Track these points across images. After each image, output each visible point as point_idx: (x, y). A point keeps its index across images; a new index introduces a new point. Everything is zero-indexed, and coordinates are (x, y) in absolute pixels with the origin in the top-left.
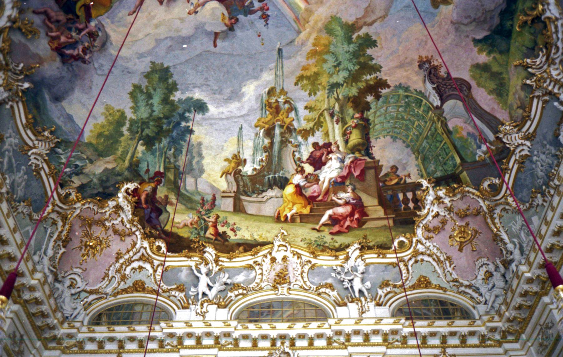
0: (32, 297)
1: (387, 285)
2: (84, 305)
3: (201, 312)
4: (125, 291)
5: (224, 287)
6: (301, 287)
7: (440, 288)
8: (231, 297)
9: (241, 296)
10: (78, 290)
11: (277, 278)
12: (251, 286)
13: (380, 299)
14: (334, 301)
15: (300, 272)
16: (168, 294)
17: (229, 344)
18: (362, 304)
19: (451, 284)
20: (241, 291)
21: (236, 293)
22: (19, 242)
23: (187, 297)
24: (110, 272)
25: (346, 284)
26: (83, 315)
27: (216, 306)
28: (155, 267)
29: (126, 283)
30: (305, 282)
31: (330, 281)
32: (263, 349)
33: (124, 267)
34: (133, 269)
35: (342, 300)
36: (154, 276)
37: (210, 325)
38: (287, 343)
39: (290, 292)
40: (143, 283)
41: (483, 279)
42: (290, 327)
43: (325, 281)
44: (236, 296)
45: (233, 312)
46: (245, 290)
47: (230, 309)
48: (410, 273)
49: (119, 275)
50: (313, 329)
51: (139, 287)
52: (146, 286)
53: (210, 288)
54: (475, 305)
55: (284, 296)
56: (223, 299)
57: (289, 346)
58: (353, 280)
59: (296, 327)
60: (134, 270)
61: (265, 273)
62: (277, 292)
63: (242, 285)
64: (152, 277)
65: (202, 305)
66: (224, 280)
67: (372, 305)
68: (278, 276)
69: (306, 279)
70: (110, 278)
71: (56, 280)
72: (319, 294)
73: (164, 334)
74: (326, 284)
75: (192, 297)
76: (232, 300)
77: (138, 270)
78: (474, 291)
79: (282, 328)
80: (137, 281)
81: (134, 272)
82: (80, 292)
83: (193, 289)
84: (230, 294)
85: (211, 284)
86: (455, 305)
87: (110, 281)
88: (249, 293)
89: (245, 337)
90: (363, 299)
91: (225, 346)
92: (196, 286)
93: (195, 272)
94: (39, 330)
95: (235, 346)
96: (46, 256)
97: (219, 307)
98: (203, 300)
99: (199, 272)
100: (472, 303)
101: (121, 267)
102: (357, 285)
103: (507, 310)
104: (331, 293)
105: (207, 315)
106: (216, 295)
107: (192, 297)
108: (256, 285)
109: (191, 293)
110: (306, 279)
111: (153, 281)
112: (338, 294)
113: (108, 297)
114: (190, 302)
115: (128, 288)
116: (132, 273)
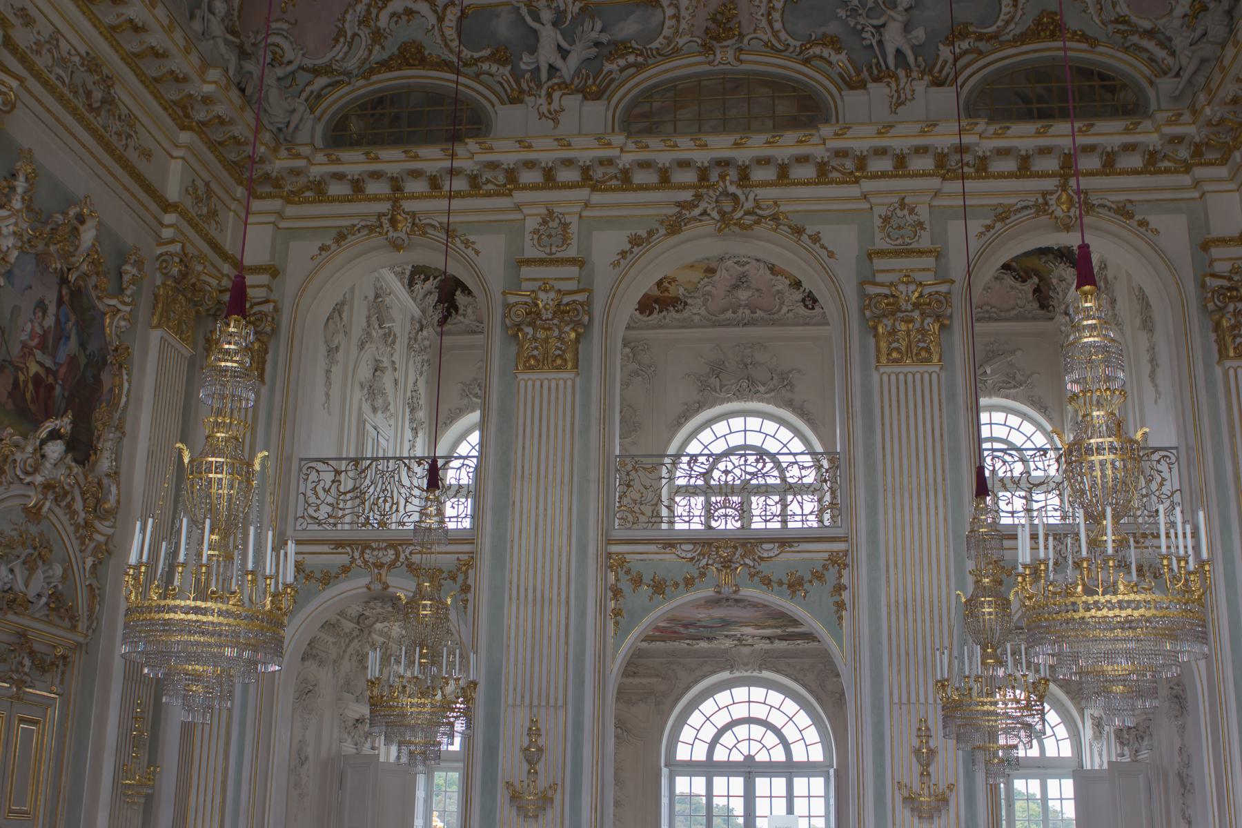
0: (211, 116)
1: (964, 35)
2: (306, 100)
3: (550, 112)
4: (385, 65)
5: (594, 51)
6: (766, 44)
7: (1084, 38)
8: (611, 72)
9: (632, 70)
10: (290, 68)
11: (712, 26)
12: (655, 45)
13: (942, 68)
14: (840, 75)
15: (763, 10)
16: (474, 69)
17: (611, 179)
18: (898, 85)
19: (1111, 28)
20: (631, 59)
21: (622, 62)
22: (166, 22)
23: (517, 75)
24: (347, 25)
25: (869, 37)
26: (310, 123)
27: (580, 96)
28: (439, 10)
29: (383, 48)
30: (775, 34)
31: (832, 28)
32: (683, 187)
33: (374, 11)
34: (394, 14)
35: (859, 72)
36: (441, 30)
37: (569, 145)
38: (733, 174)
39: (743, 57)
40: (420, 48)
41: (1185, 16)
42: (737, 145)
43: (824, 29)
44: (622, 70)
45: (617, 106)
46: (641, 54)
47: (609, 101)
48: (1020, 6)
49: (367, 31)
50: (788, 145)
51: (411, 55)
52: (426, 53)
53: (564, 54)
54: (1153, 78)
55: (729, 67)
56: (595, 78)
57: (736, 179)
58: (884, 25)
59: (750, 143)
60: (395, 19)
61: (683, 13)
62: (711, 57)
63: (635, 45)
64: (436, 32)
65: (549, 96)
66: (594, 35)
67: (920, 86)
68: (714, 20)
69: (778, 26)
70: (349, 39)
71: (243, 54)
72: (806, 62)
73: (476, 163)
74: (825, 35)
75: (528, 75)
76: (613, 80)
77: (404, 18)
78: (1160, 44)
79: (720, 146)
80: (405, 44)
81: (396, 23)
82: (293, 73)
83: (526, 58)
84: (608, 67)
85: (565, 45)
86: (1114, 79)
87: (351, 44)
88: (650, 61)
89: (644, 165)
90: (901, 73)
91: (604, 182)
92: (533, 50)
93: (528, 19)
94: (234, 168)
95: (623, 183)
96: (214, 14)
97: (585, 98)
98: (550, 83)
99: (537, 19)
100: (1147, 72)
101: (368, 11)
102: (893, 38)
103: (1209, 104)
104: (834, 58)
105: (562, 117)
106: (579, 70)
107: (528, 75)
108: (664, 41)
109: (523, 66)
110: (778, 26)
111: (439, 40)
112: (850, 60)
113: (353, 80)
114: (524, 86)
115: (391, 58)
116: (393, 26)
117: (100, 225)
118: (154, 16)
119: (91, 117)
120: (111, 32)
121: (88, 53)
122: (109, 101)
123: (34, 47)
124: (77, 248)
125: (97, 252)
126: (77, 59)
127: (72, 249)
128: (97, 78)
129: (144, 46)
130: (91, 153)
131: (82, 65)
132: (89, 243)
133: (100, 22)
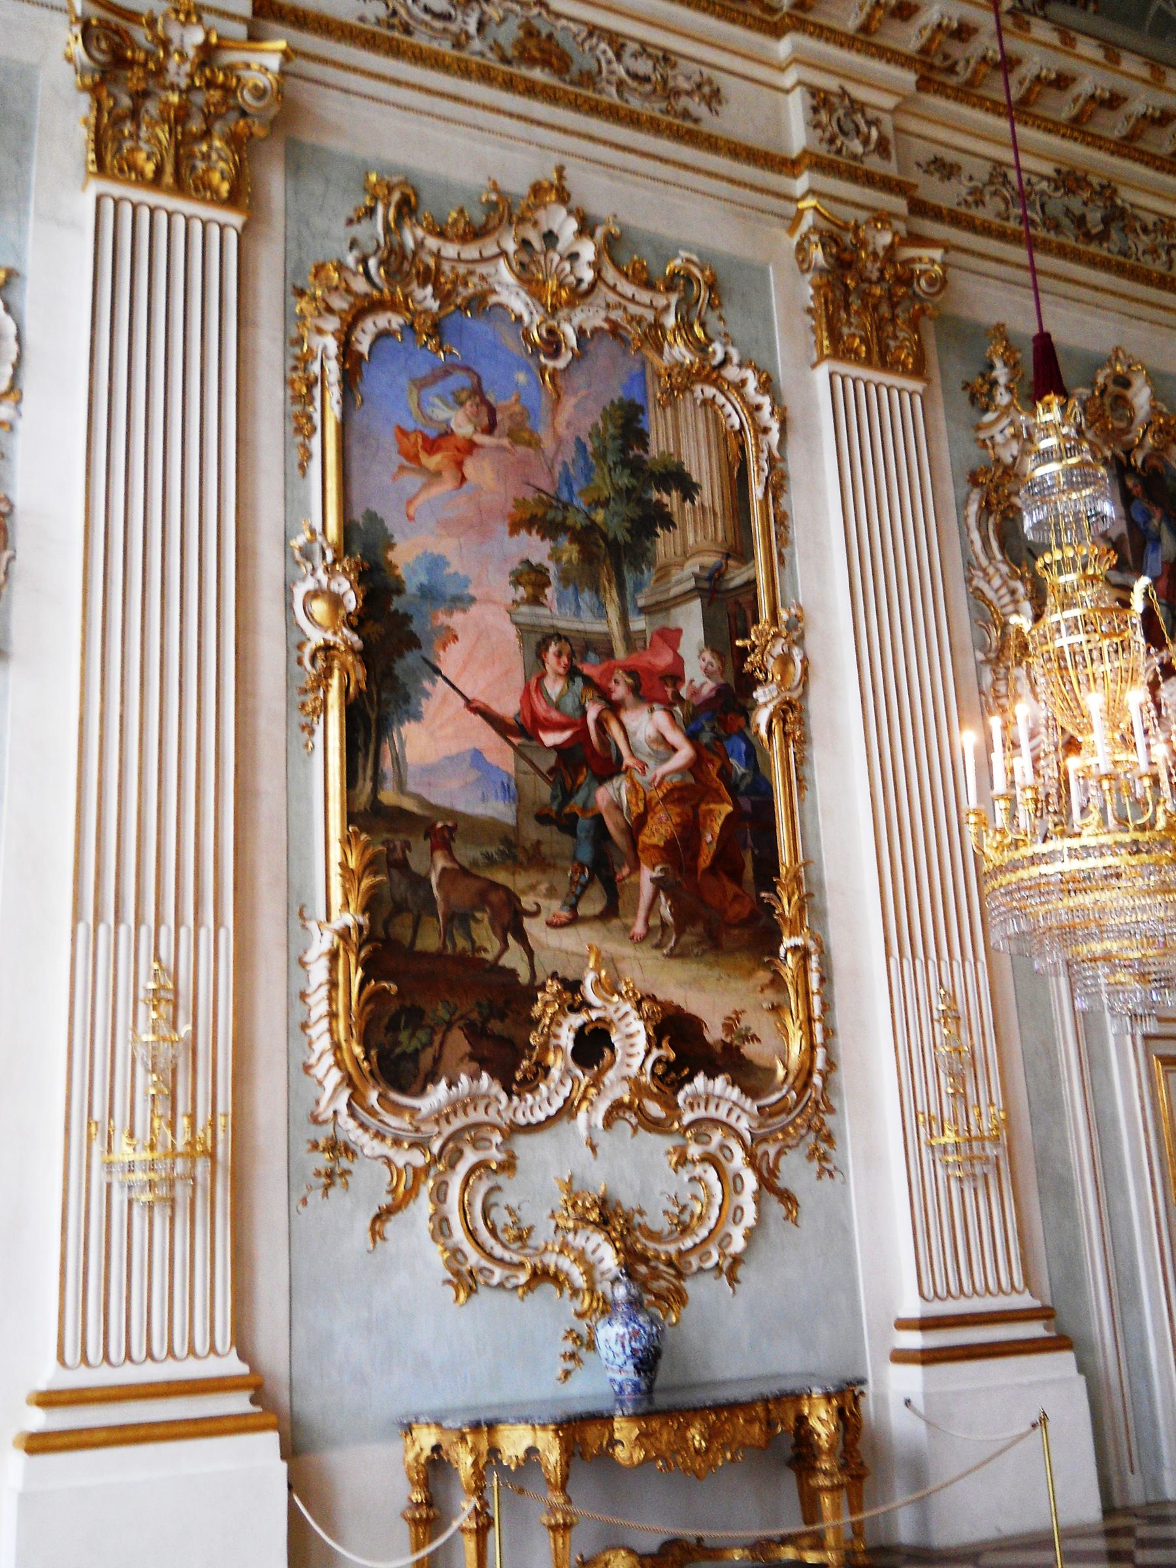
117: (1154, 378)
118: (1125, 74)
119: (1093, 248)
120: (1076, 128)
121: (1058, 171)
122: (1117, 216)
123: (970, 199)
124: (1131, 420)
125: (1161, 413)
126: (1044, 185)
127: (1123, 425)
128: (1086, 195)
129: (1133, 120)
130: (1113, 293)
131: (1057, 189)
132: (1147, 408)
133: (1055, 123)
